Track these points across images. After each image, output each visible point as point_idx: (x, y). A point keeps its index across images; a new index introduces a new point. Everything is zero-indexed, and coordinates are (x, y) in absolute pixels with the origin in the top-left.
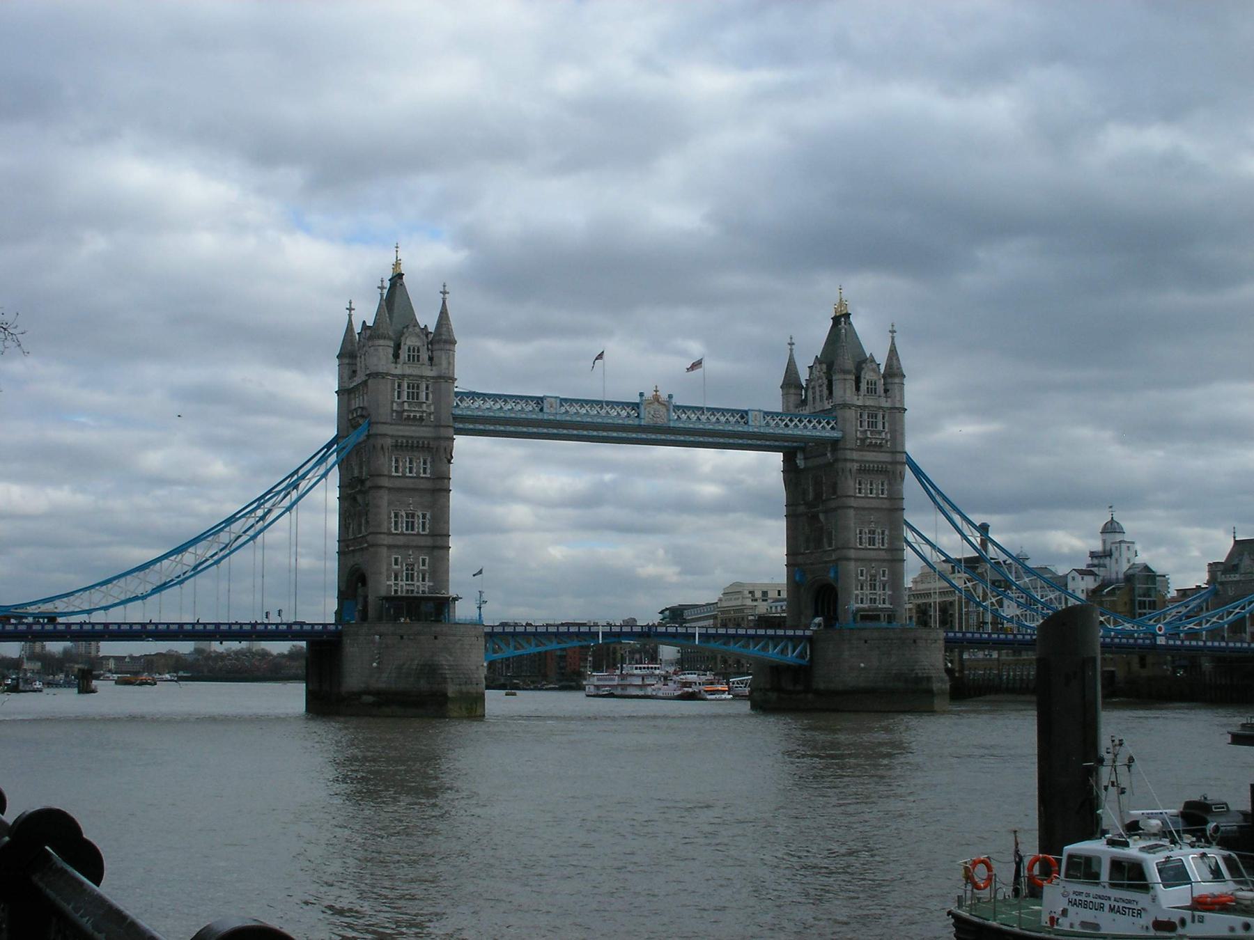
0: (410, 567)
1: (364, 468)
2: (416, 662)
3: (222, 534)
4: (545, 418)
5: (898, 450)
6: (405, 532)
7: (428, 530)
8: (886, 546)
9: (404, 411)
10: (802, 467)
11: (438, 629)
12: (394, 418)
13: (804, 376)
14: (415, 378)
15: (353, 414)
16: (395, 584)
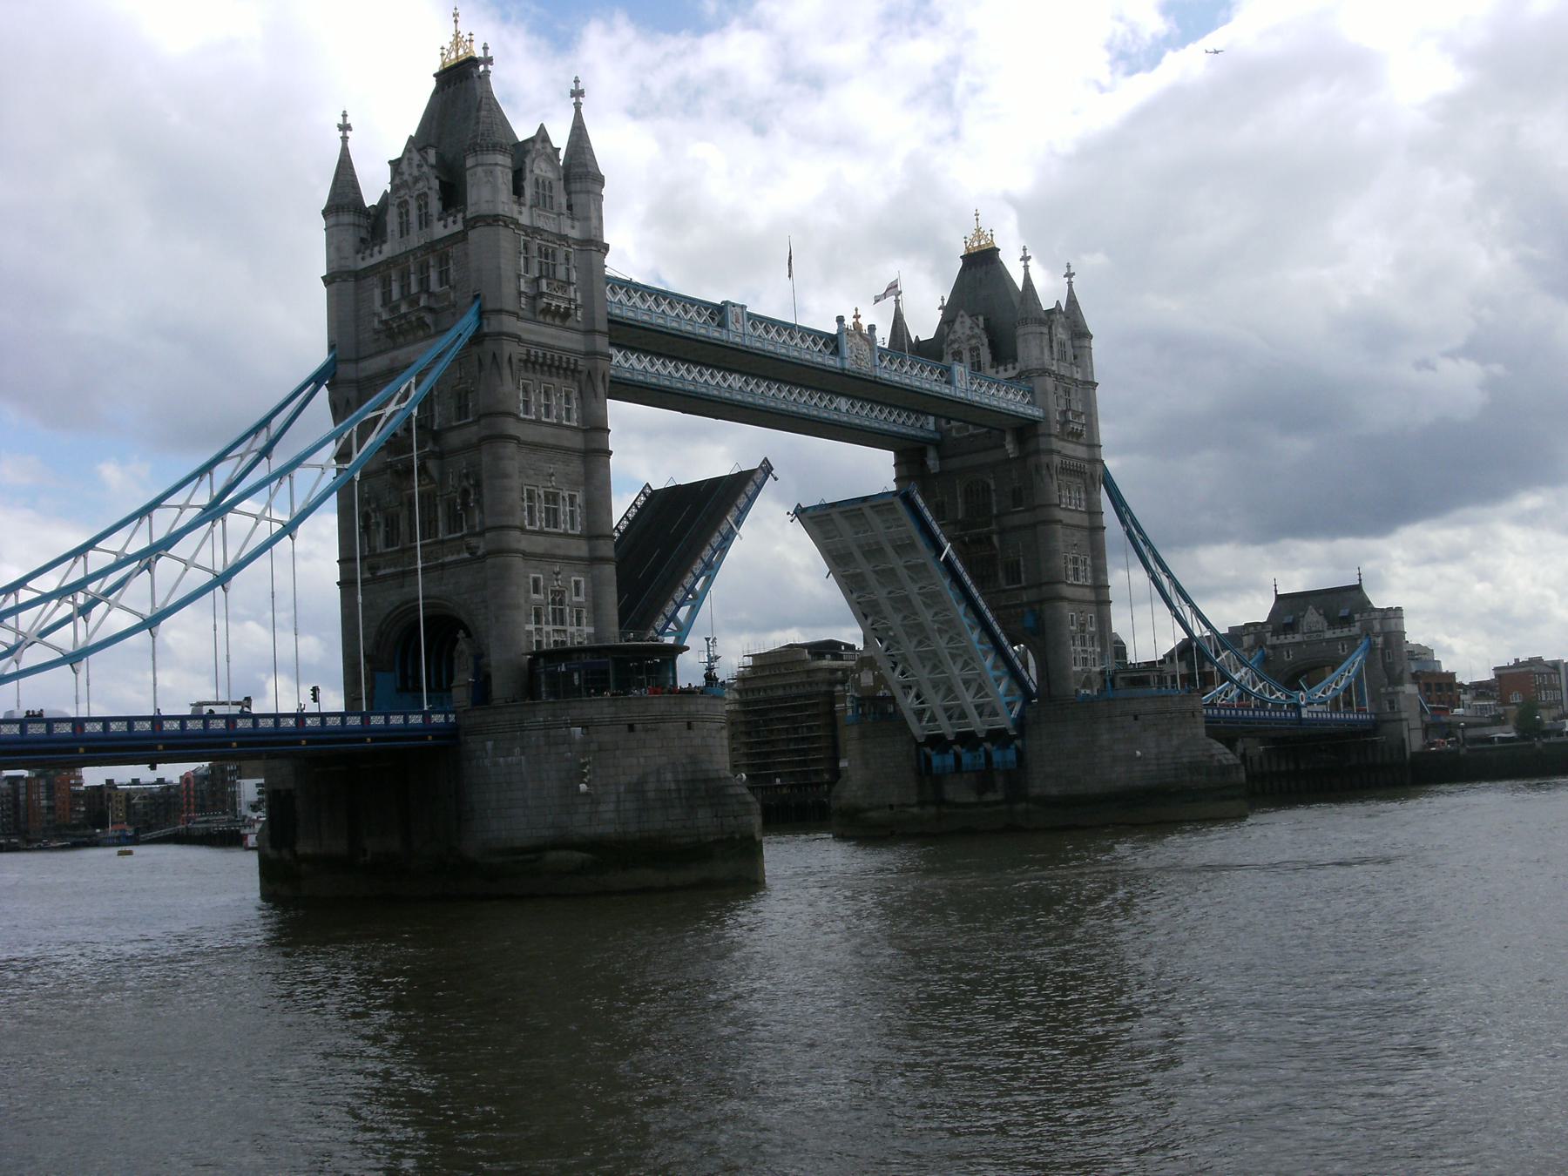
0: (558, 598)
1: (436, 407)
2: (669, 776)
3: (230, 516)
4: (731, 339)
5: (1096, 442)
6: (546, 529)
7: (578, 530)
8: (1089, 582)
9: (542, 294)
10: (937, 470)
11: (693, 708)
12: (523, 306)
13: (913, 340)
14: (551, 238)
15: (397, 307)
16: (536, 629)
